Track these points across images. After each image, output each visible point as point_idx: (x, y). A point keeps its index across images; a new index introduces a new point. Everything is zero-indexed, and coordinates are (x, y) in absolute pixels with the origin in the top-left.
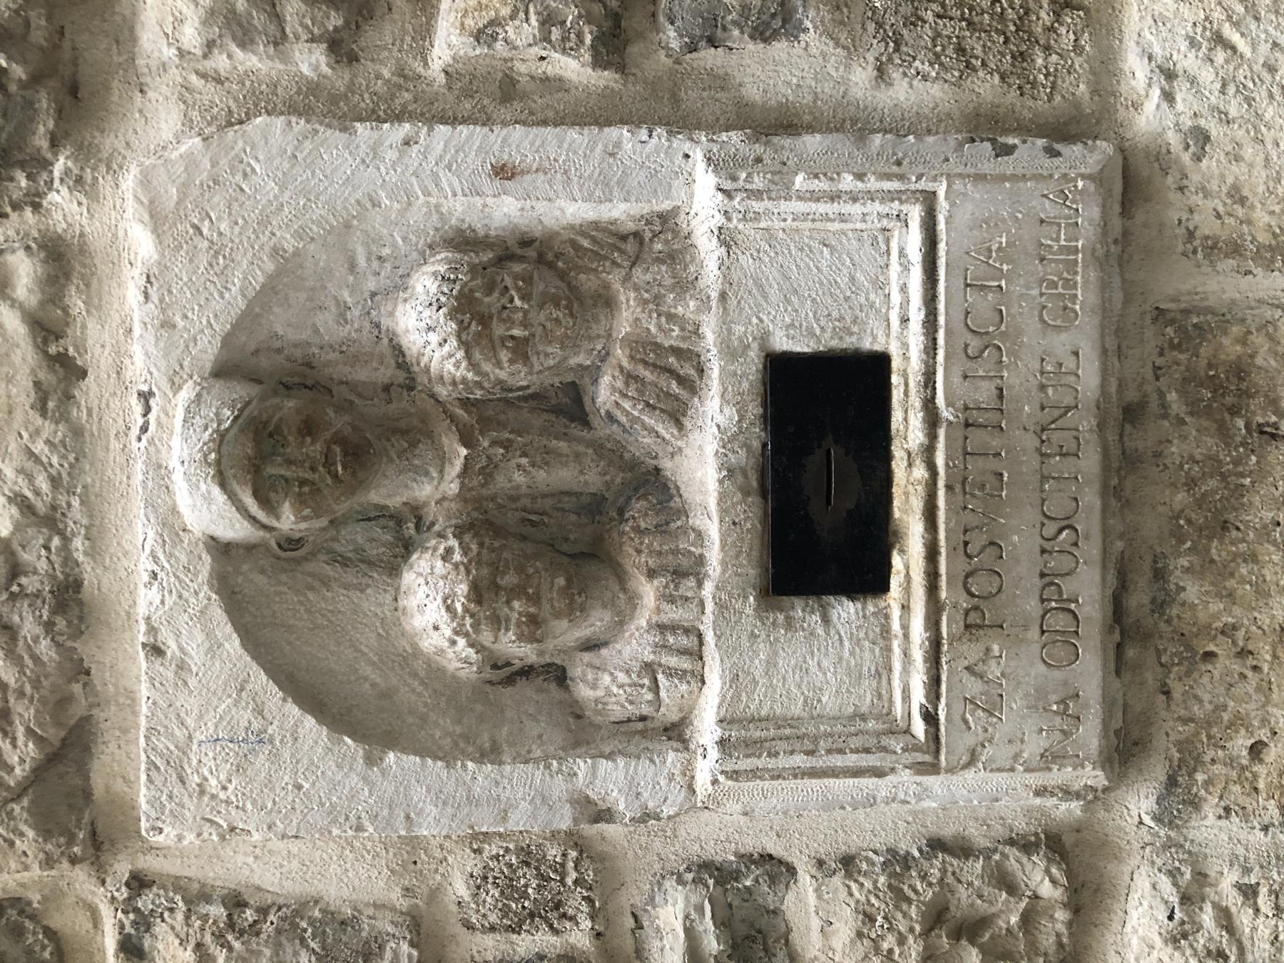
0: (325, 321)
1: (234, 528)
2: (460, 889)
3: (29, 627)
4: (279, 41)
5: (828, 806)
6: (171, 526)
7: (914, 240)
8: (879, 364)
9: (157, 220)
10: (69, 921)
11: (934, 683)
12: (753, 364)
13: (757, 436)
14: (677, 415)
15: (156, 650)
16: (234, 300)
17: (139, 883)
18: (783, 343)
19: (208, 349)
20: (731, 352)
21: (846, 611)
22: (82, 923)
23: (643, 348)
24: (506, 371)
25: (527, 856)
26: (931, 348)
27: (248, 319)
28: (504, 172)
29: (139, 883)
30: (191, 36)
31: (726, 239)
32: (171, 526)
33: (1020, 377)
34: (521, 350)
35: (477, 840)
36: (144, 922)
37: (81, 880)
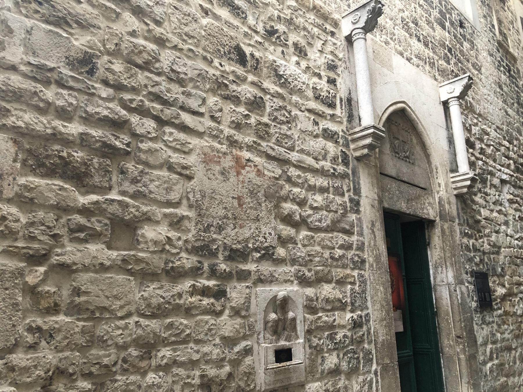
0: (290, 305)
1: (278, 297)
2: (251, 320)
3: (270, 278)
4: (306, 301)
5: (259, 360)
6: (279, 292)
7: (300, 362)
8: (292, 360)
9: (297, 291)
10: (248, 281)
11: (271, 369)
12: (291, 347)
13: (286, 348)
14: (286, 340)
15: (271, 290)
16: (292, 297)
17: (252, 287)
18: (292, 350)
19: (290, 295)
20: (292, 344)
21: (274, 359)
22: (248, 281)
23: (291, 336)
24: (288, 322)
25: (254, 327)
26: (294, 365)
27: (292, 299)
28: (301, 322)
29: (252, 287)
30: (306, 293)
31: (299, 343)
32: (279, 292)
33: (292, 375)
34: (291, 324)
35: (256, 321)
36: (249, 288)
37: (252, 282)
